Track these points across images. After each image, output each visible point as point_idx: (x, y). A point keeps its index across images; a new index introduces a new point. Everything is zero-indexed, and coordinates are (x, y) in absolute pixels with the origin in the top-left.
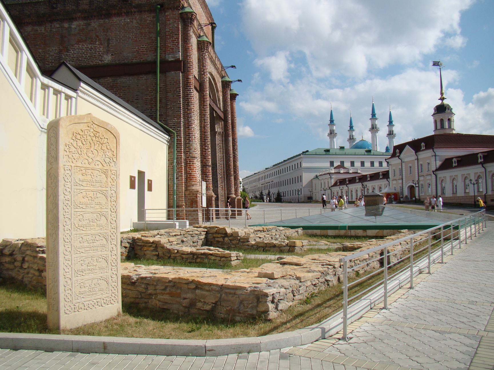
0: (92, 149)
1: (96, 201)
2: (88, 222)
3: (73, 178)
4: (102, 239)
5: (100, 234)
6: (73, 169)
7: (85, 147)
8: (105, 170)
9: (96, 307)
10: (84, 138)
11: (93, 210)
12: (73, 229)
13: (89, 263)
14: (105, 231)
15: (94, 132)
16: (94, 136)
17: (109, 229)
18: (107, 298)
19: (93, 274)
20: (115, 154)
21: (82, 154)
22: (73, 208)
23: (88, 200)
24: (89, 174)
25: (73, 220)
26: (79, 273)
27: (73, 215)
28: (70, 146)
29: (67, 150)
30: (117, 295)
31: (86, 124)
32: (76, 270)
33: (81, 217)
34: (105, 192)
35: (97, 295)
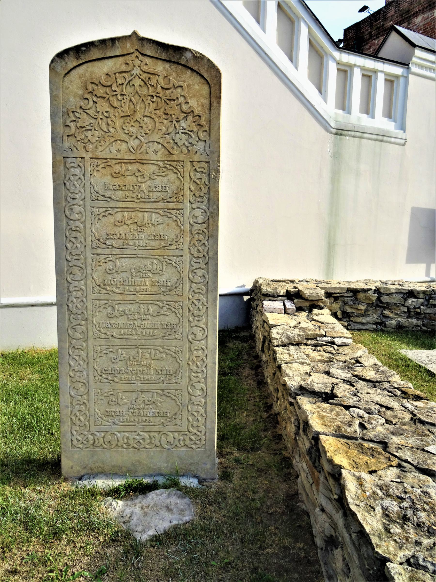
0: (138, 116)
1: (150, 231)
2: (130, 276)
3: (88, 184)
4: (165, 313)
5: (160, 304)
6: (87, 165)
7: (117, 114)
8: (174, 164)
9: (148, 446)
10: (114, 93)
11: (141, 252)
12: (90, 290)
13: (131, 359)
14: (176, 298)
15: (144, 76)
16: (142, 84)
17: (186, 294)
18: (176, 434)
19: (139, 382)
20: (203, 121)
21: (111, 130)
22: (89, 247)
23: (128, 230)
24: (130, 173)
25: (89, 271)
26: (104, 376)
27: (89, 261)
28: (77, 114)
29: (72, 125)
30: (203, 433)
31: (121, 59)
32: (96, 367)
33: (110, 265)
34: (174, 212)
35: (151, 424)
